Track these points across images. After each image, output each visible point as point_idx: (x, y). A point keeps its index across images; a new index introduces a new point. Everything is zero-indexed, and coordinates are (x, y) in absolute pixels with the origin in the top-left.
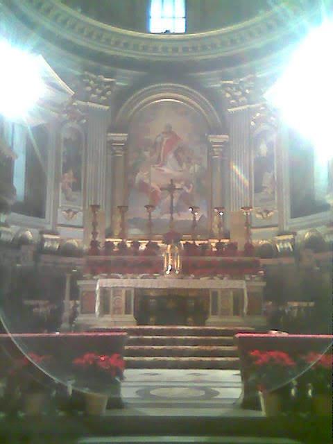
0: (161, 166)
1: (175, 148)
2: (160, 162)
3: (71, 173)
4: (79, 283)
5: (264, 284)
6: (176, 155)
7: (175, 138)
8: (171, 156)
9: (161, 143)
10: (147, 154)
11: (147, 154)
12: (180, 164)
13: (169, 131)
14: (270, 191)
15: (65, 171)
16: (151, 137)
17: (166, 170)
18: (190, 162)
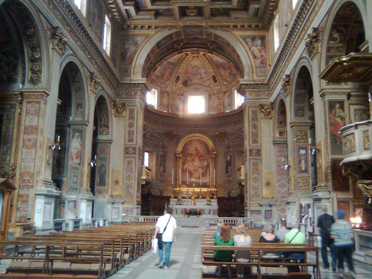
0: (194, 162)
1: (198, 156)
2: (193, 161)
3: (162, 166)
4: (169, 206)
5: (218, 207)
6: (198, 157)
7: (198, 153)
8: (197, 159)
9: (193, 154)
10: (188, 158)
11: (188, 158)
12: (200, 161)
13: (196, 150)
14: (230, 173)
15: (160, 166)
16: (190, 152)
17: (195, 164)
18: (204, 161)
